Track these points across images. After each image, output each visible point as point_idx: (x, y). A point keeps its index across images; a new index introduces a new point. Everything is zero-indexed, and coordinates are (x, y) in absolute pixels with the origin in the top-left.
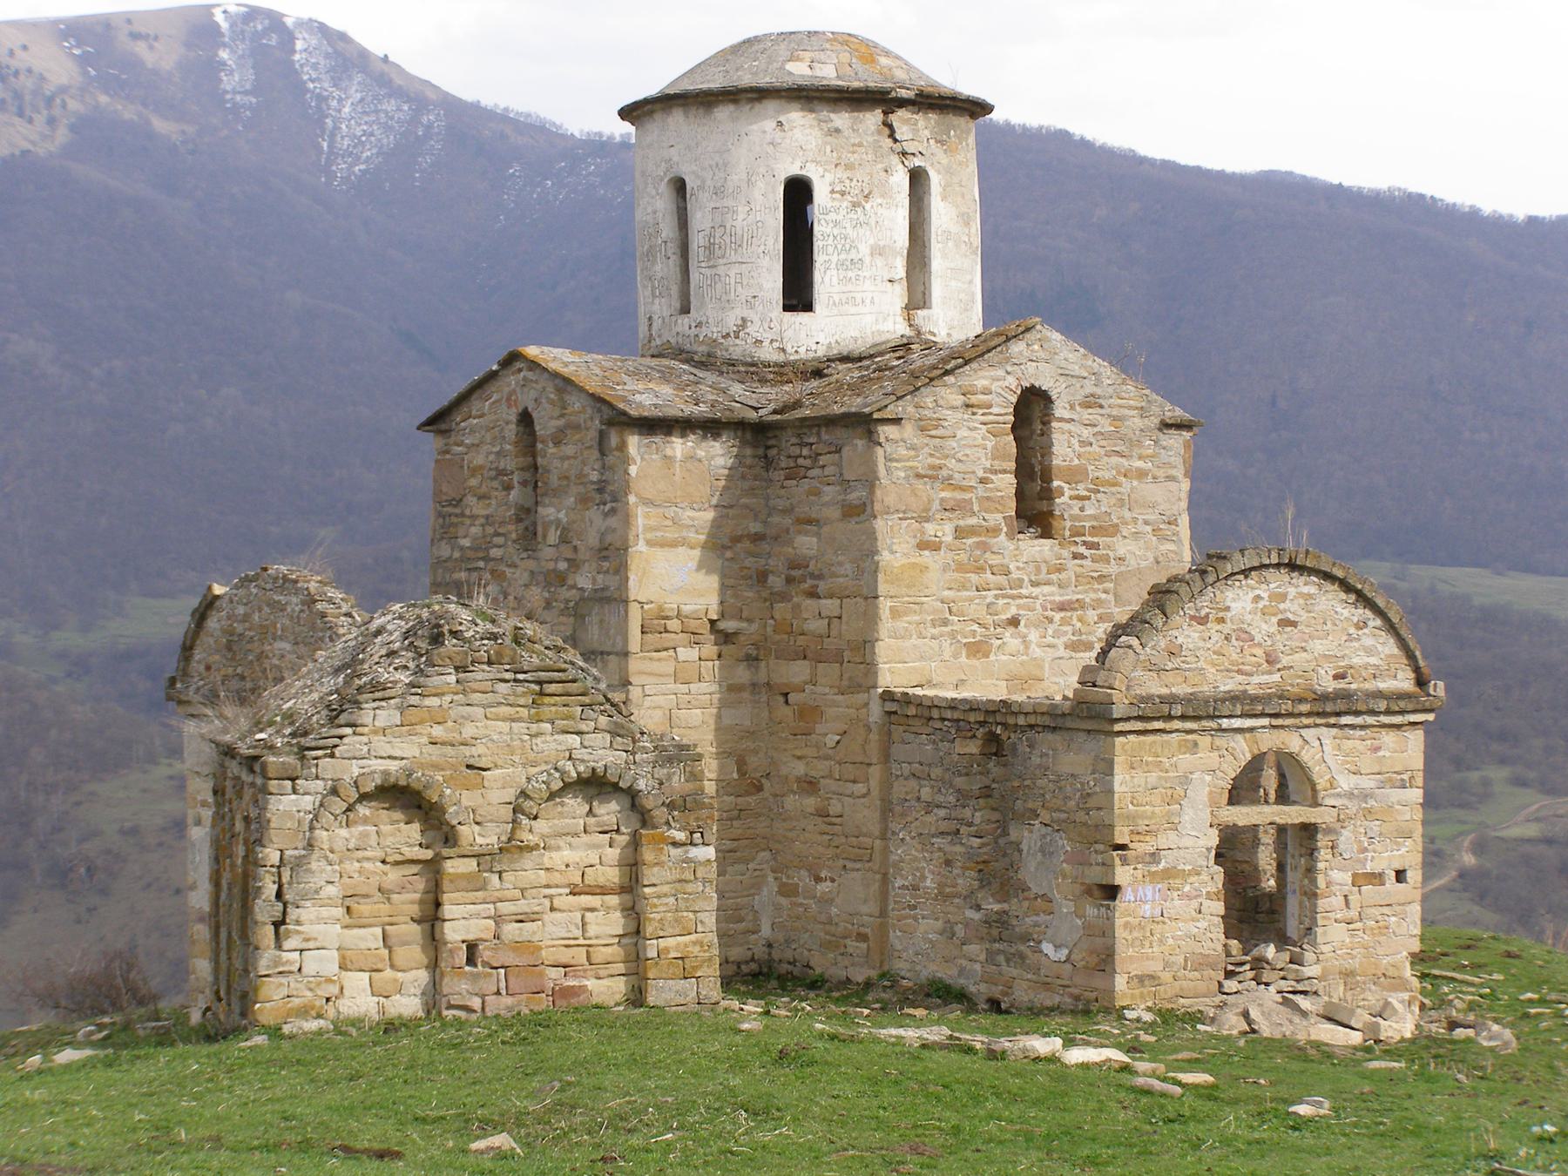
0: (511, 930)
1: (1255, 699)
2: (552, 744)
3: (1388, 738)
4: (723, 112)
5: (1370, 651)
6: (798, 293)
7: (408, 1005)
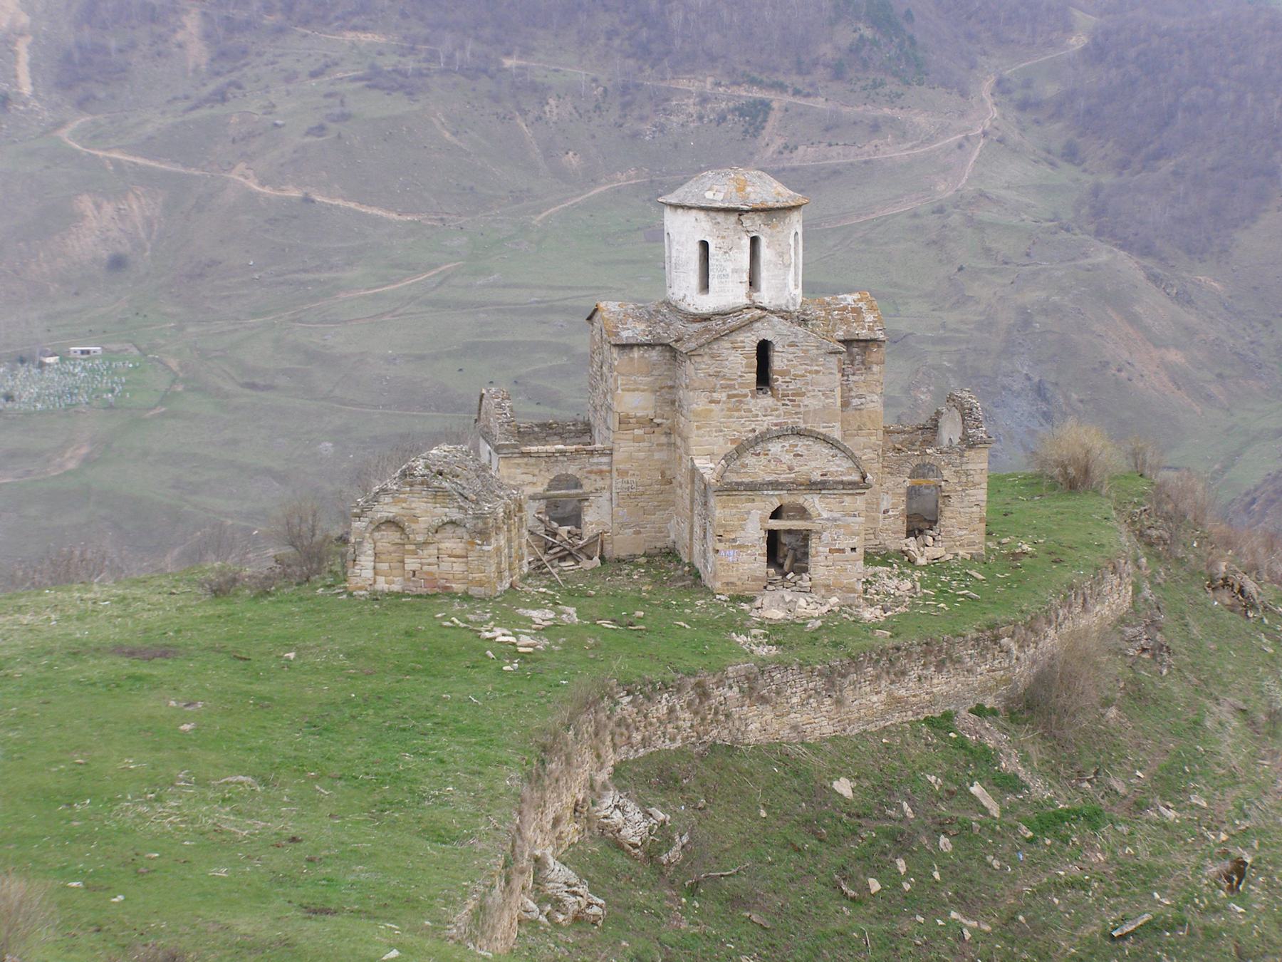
0: (425, 568)
1: (781, 484)
2: (439, 510)
3: (847, 499)
4: (680, 211)
5: (838, 466)
6: (705, 287)
7: (396, 588)
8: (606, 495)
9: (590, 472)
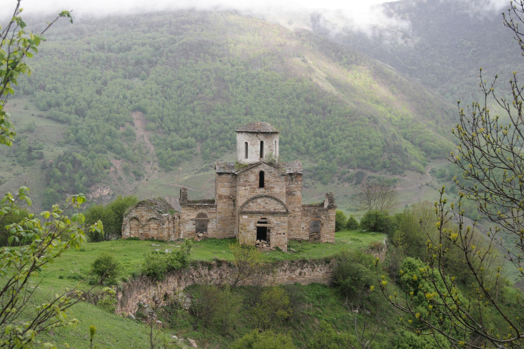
2: (150, 214)
3: (282, 217)
6: (247, 157)
8: (215, 220)
9: (210, 212)
